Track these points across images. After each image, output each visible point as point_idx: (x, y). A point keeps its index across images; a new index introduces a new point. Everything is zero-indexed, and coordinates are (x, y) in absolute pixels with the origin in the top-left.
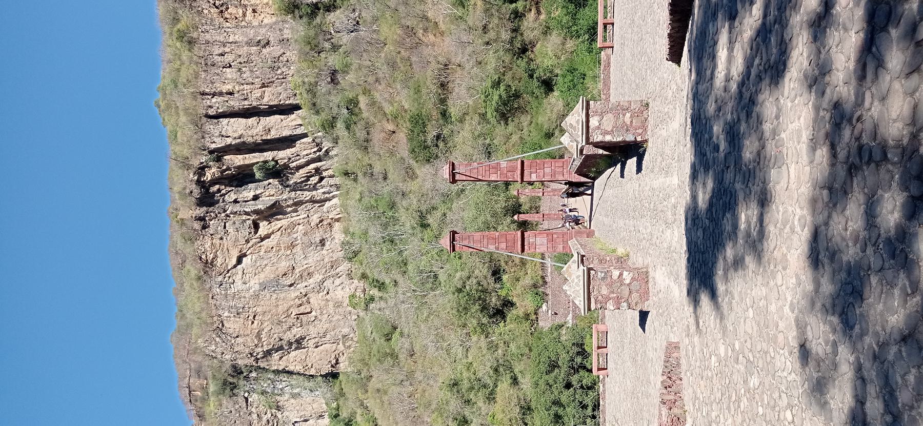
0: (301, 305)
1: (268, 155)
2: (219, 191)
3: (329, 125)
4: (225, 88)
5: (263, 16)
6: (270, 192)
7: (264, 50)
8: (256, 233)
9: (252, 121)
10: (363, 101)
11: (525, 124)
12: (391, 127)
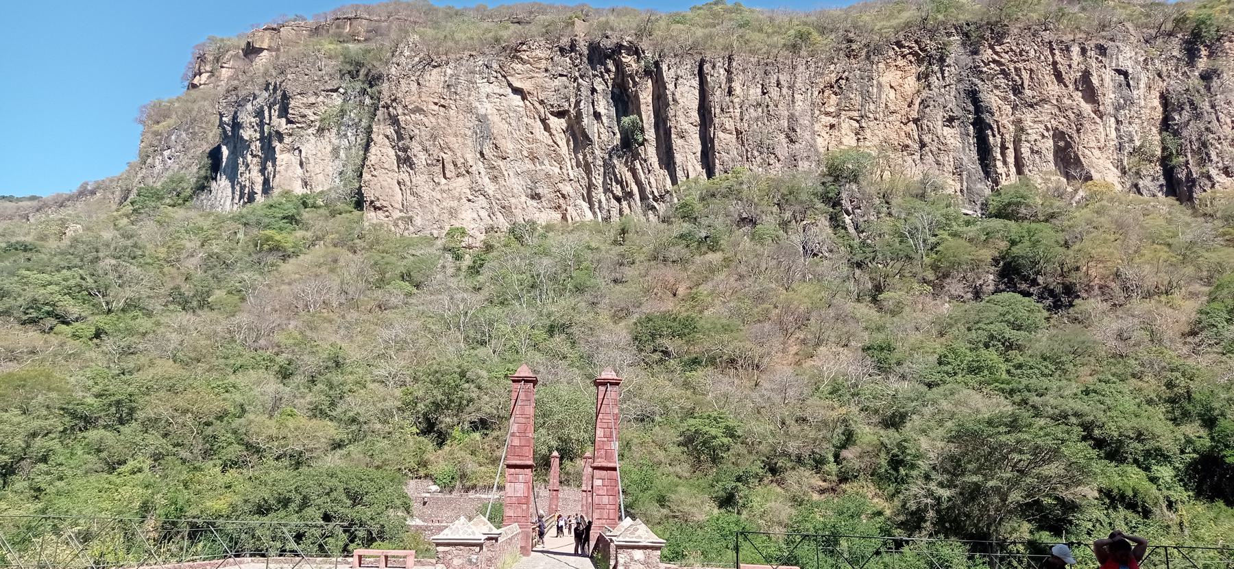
0: (455, 165)
1: (651, 134)
2: (608, 71)
3: (686, 213)
4: (737, 86)
5: (827, 136)
6: (604, 133)
7: (783, 136)
8: (552, 113)
9: (695, 116)
10: (715, 257)
11: (678, 469)
12: (682, 291)
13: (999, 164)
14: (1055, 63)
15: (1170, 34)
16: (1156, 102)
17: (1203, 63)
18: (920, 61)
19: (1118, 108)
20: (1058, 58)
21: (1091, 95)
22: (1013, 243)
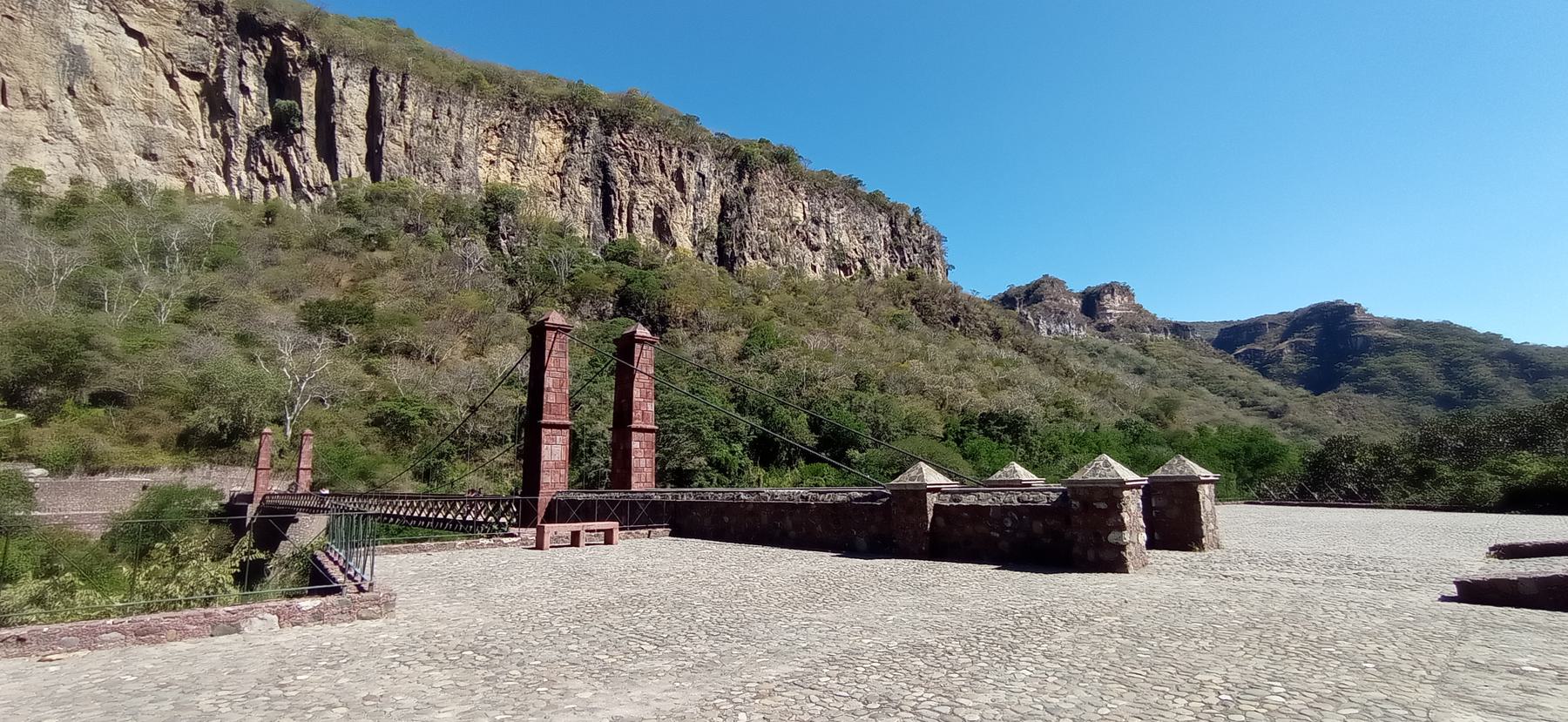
0: (25, 93)
1: (310, 124)
2: (263, 48)
3: (349, 207)
4: (409, 103)
6: (252, 107)
8: (183, 72)
9: (362, 120)
10: (383, 256)
11: (372, 447)
17: (746, 182)
18: (567, 129)
19: (696, 199)
21: (681, 186)
22: (629, 282)
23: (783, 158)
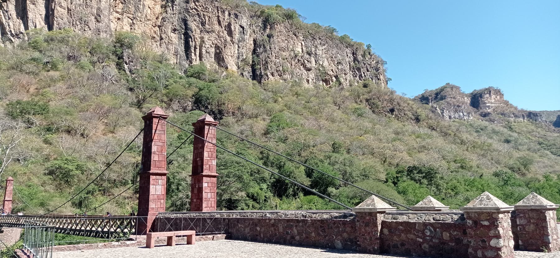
3: (35, 46)
5: (116, 23)
7: (93, 18)
12: (32, 90)
13: (193, 54)
14: (218, 17)
15: (259, 17)
16: (252, 42)
17: (268, 31)
19: (239, 41)
20: (220, 15)
21: (230, 33)
22: (200, 89)
23: (289, 16)
